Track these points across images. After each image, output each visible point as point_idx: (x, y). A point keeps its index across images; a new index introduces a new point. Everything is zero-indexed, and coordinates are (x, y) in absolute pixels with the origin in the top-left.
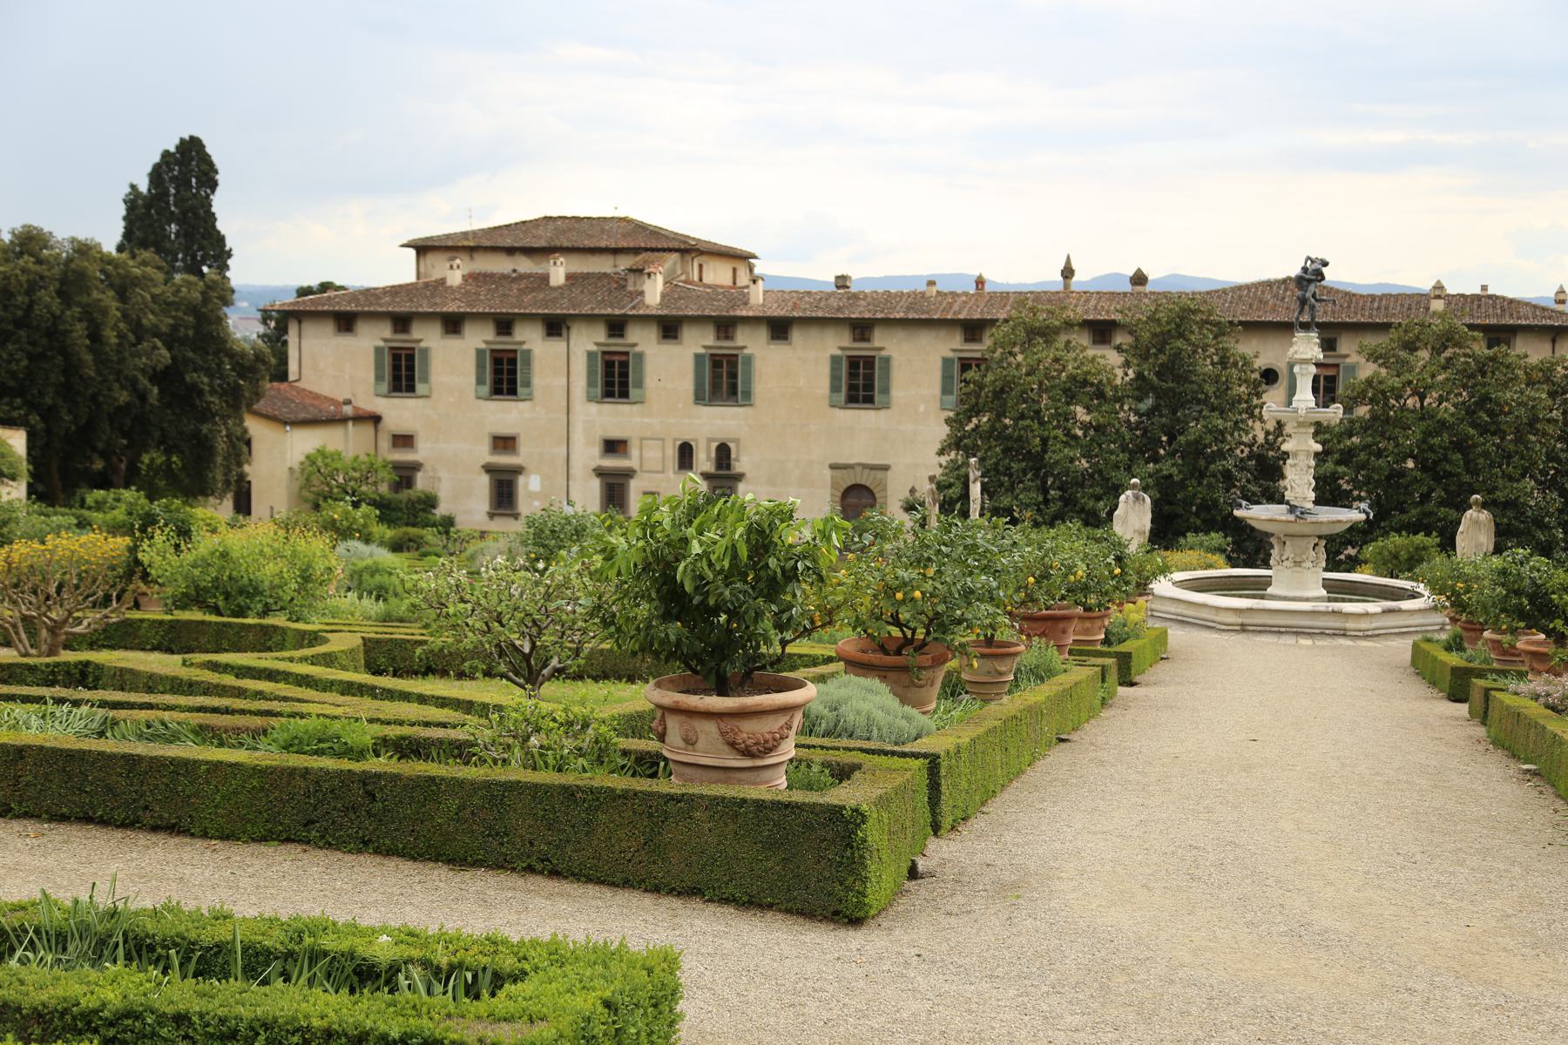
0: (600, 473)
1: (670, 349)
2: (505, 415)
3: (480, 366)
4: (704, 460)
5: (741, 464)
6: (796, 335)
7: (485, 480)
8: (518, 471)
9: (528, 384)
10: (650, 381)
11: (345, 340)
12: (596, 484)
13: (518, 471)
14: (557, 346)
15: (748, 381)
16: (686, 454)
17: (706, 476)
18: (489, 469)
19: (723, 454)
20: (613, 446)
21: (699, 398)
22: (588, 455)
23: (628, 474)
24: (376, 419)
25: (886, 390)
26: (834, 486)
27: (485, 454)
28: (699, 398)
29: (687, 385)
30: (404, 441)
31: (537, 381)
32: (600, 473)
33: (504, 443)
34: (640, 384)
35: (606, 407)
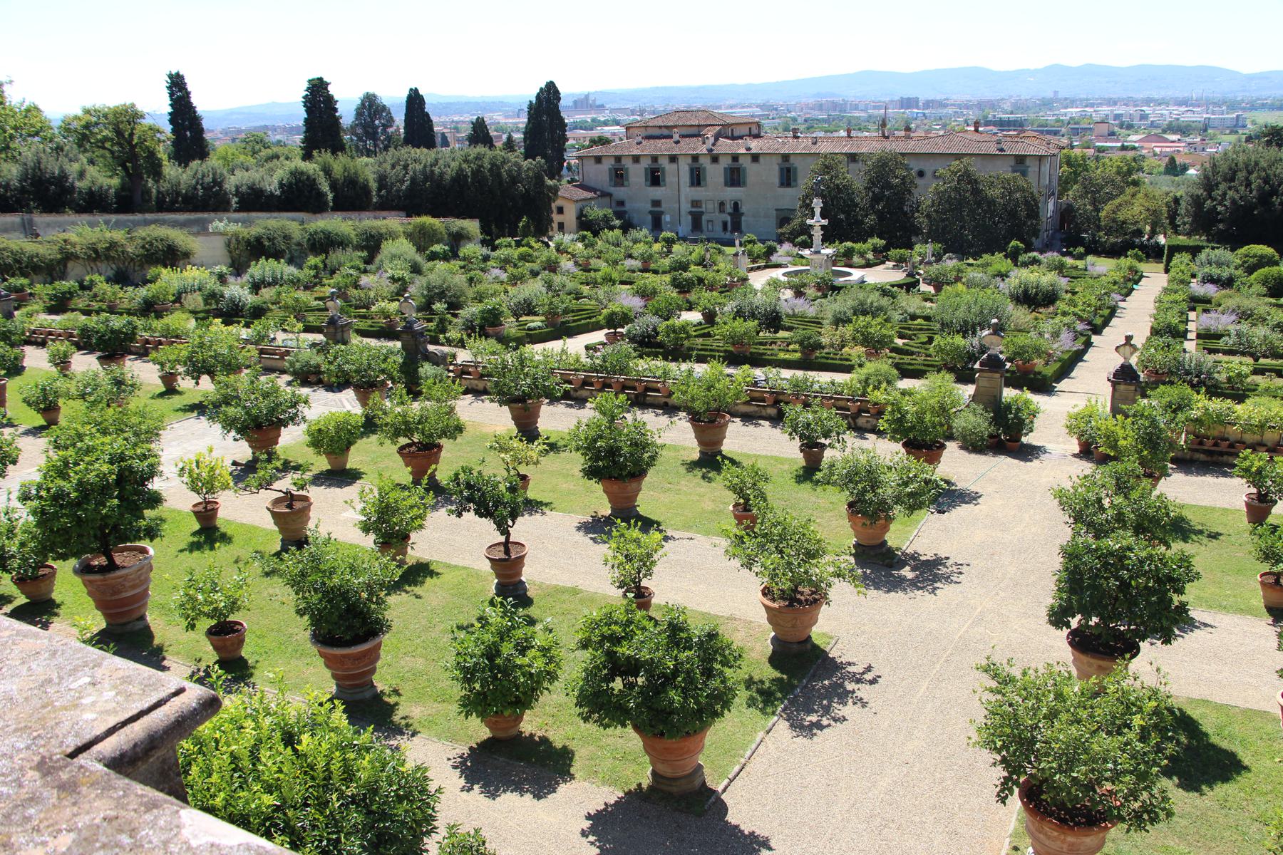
0: (691, 213)
1: (714, 166)
2: (656, 192)
3: (646, 174)
4: (729, 209)
5: (743, 209)
6: (761, 159)
7: (650, 217)
8: (662, 213)
9: (664, 180)
10: (708, 179)
11: (599, 166)
12: (690, 217)
13: (662, 213)
14: (674, 166)
15: (745, 177)
16: (722, 204)
17: (729, 214)
18: (651, 212)
19: (736, 206)
20: (695, 203)
21: (726, 185)
22: (686, 207)
23: (702, 213)
24: (610, 195)
25: (795, 180)
26: (777, 217)
27: (649, 207)
28: (726, 185)
29: (722, 180)
30: (621, 203)
31: (667, 180)
32: (691, 213)
33: (656, 203)
34: (705, 179)
35: (693, 189)
